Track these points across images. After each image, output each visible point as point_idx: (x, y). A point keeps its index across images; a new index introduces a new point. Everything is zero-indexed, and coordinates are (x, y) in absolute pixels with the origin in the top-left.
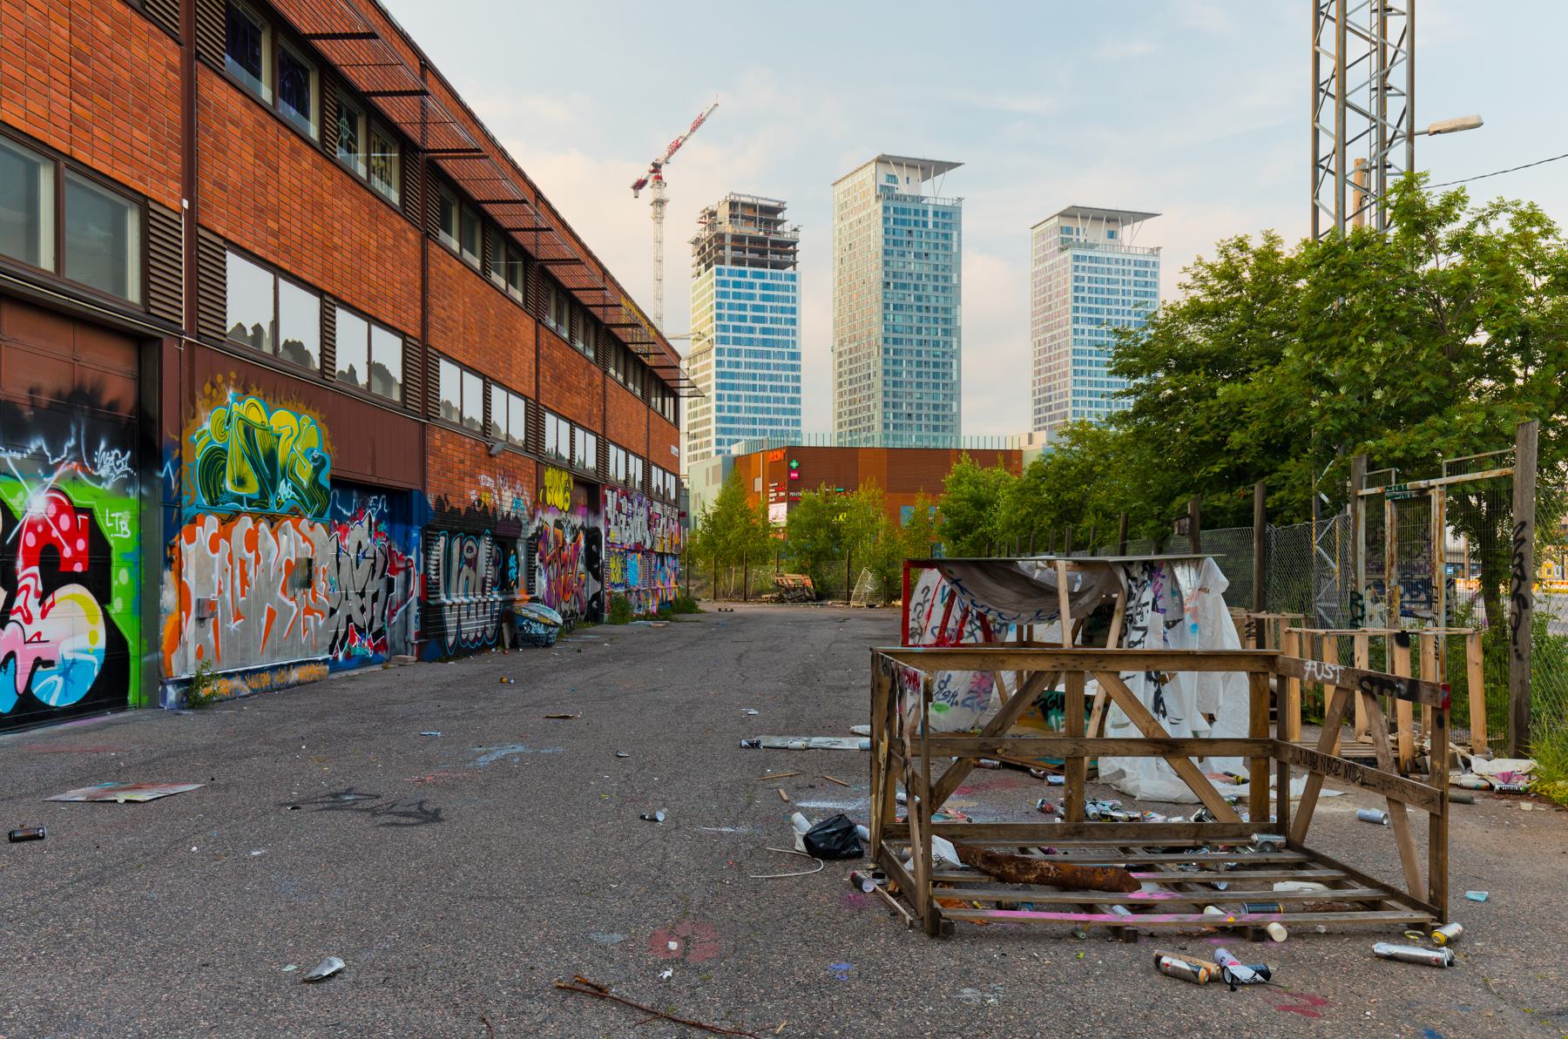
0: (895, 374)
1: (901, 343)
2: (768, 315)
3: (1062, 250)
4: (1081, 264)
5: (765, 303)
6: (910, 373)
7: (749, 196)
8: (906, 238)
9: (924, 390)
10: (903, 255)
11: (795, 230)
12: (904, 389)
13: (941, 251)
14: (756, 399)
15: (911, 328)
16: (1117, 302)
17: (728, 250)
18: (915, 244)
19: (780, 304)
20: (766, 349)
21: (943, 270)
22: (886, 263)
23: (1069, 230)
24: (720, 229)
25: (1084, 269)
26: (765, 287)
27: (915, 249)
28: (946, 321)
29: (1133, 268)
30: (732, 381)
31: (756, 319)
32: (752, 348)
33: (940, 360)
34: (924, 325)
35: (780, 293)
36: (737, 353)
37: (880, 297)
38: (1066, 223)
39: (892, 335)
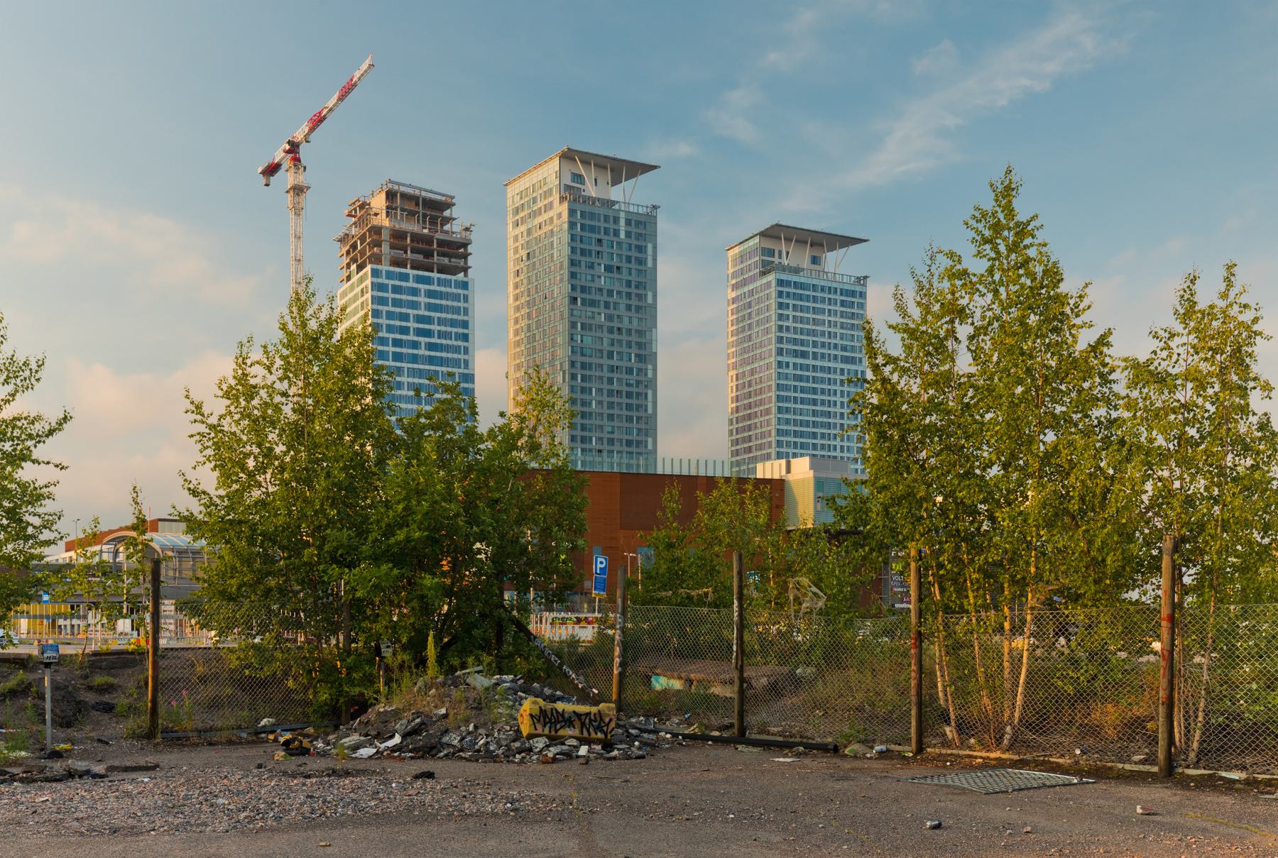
1: (590, 369)
2: (435, 327)
3: (763, 274)
4: (785, 290)
5: (432, 314)
6: (600, 403)
7: (410, 186)
8: (594, 248)
9: (616, 423)
10: (592, 266)
11: (467, 229)
12: (593, 421)
13: (633, 266)
15: (601, 351)
16: (823, 334)
17: (385, 248)
18: (605, 255)
19: (449, 316)
20: (433, 368)
21: (637, 287)
22: (573, 275)
23: (771, 253)
24: (376, 221)
25: (788, 295)
26: (430, 294)
27: (605, 261)
28: (639, 345)
29: (839, 298)
31: (420, 332)
32: (416, 366)
33: (634, 390)
34: (616, 349)
37: (566, 315)
38: (769, 244)
39: (580, 359)
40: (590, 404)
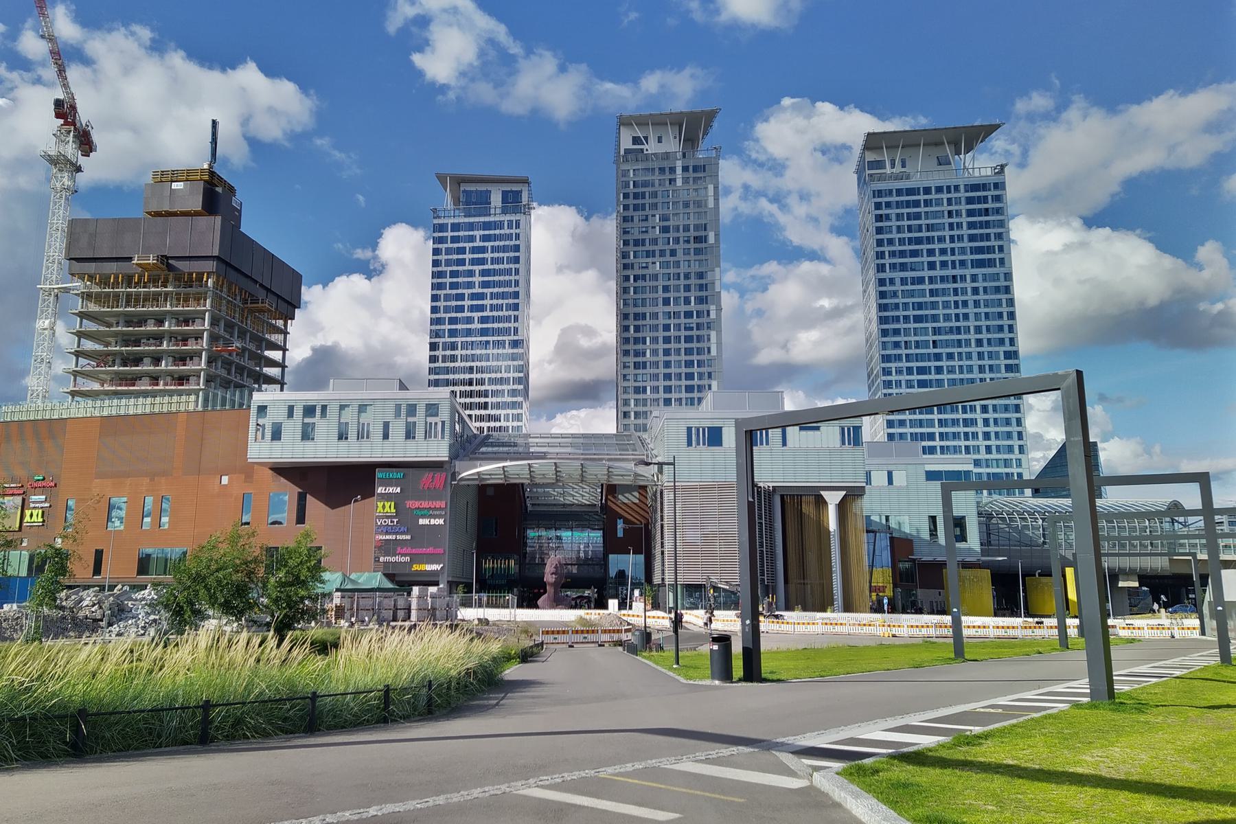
0: (637, 354)
2: (487, 302)
14: (471, 394)
26: (484, 273)
28: (701, 287)
30: (446, 377)
33: (695, 333)
36: (453, 346)
40: (644, 354)
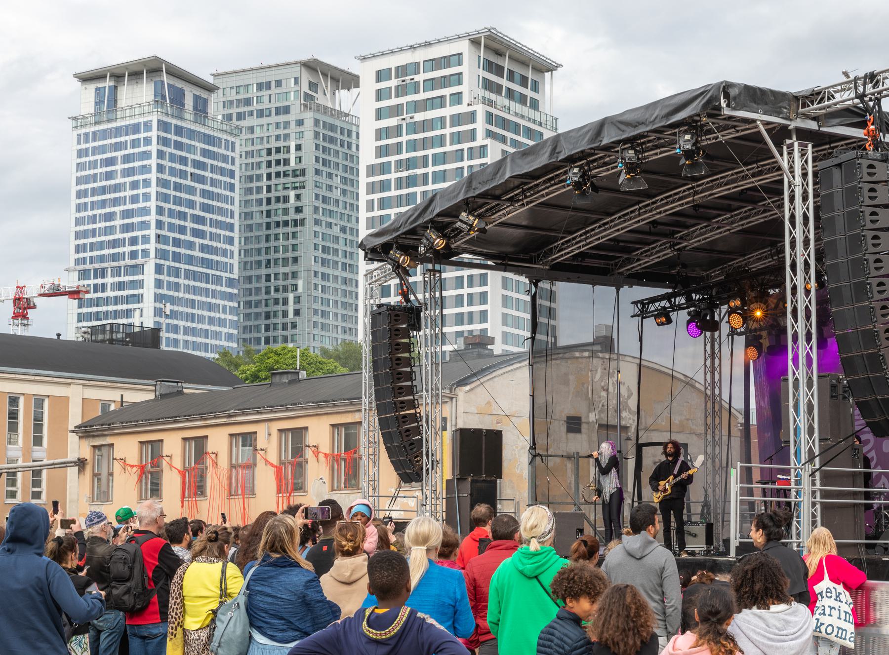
20: (205, 270)
26: (205, 194)
32: (191, 268)
35: (220, 204)
